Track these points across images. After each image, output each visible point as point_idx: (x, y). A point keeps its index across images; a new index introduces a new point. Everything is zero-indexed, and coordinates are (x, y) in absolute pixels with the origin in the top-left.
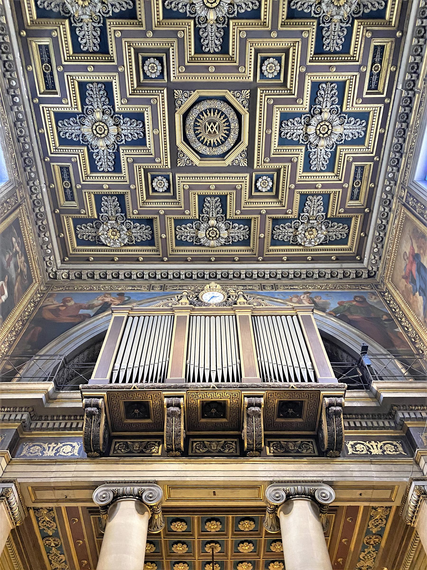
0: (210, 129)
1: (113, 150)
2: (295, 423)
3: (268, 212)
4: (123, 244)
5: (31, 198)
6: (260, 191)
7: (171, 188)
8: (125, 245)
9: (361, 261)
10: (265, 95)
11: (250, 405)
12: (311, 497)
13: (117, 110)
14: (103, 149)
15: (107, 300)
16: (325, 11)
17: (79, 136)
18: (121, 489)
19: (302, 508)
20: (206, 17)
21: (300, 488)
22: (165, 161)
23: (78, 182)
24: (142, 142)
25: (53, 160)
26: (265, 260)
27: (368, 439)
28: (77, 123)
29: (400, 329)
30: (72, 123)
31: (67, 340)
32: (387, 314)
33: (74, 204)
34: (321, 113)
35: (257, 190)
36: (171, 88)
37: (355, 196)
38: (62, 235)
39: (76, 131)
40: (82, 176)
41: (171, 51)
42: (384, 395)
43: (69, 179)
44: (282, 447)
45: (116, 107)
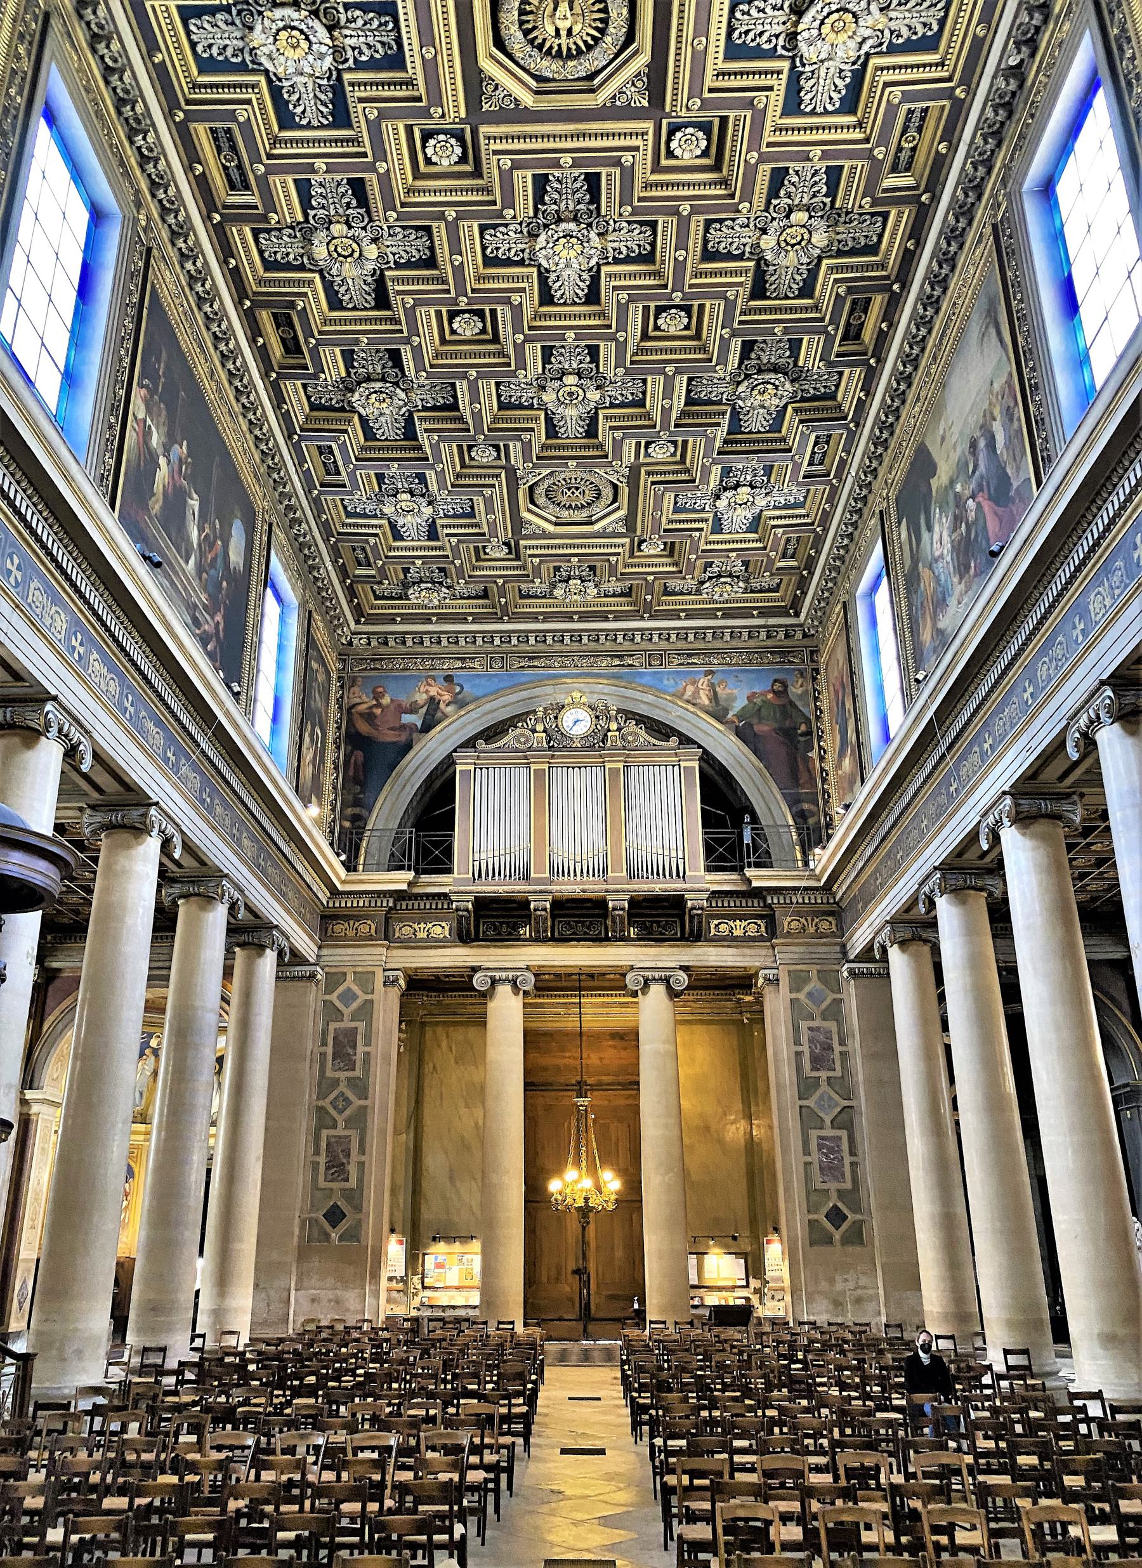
1: (329, 79)
2: (661, 916)
5: (132, 142)
7: (472, 158)
9: (797, 615)
11: (614, 909)
12: (666, 981)
15: (433, 691)
17: (242, 50)
18: (497, 975)
19: (657, 991)
21: (657, 975)
22: (455, 105)
24: (396, 61)
26: (652, 618)
27: (734, 918)
28: (233, 24)
29: (814, 754)
30: (221, 24)
31: (401, 781)
32: (808, 721)
37: (790, 552)
38: (200, 168)
39: (235, 42)
40: (263, 144)
42: (755, 884)
44: (646, 928)
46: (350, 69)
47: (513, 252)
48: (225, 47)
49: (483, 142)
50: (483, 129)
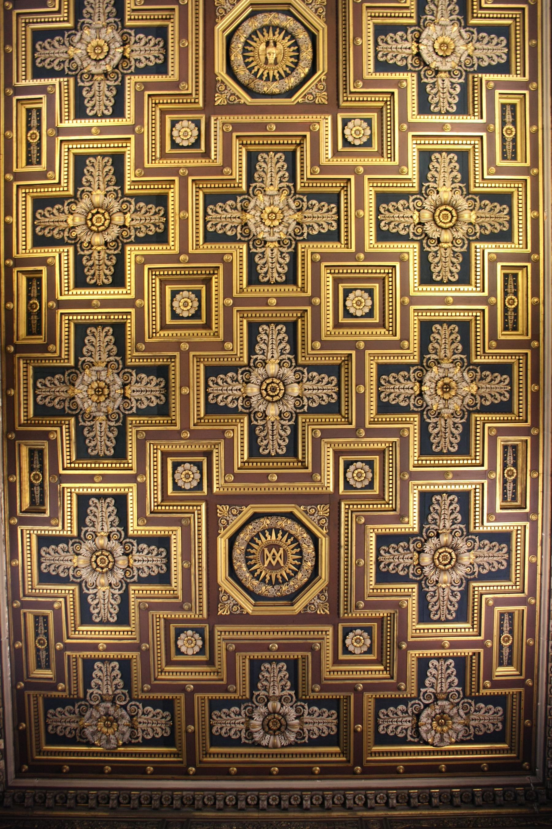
0: (270, 558)
3: (368, 688)
4: (121, 742)
6: (351, 653)
8: (124, 745)
10: (352, 512)
13: (130, 533)
14: (103, 589)
16: (430, 403)
20: (264, 411)
23: (59, 638)
25: (26, 605)
33: (48, 674)
34: (438, 536)
35: (346, 651)
36: (213, 501)
41: (215, 455)
43: (47, 634)
45: (130, 529)
46: (134, 582)
47: (233, 732)
48: (65, 728)
49: (217, 633)
50: (218, 628)
